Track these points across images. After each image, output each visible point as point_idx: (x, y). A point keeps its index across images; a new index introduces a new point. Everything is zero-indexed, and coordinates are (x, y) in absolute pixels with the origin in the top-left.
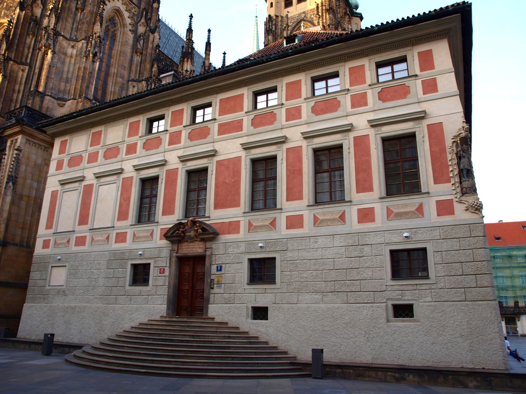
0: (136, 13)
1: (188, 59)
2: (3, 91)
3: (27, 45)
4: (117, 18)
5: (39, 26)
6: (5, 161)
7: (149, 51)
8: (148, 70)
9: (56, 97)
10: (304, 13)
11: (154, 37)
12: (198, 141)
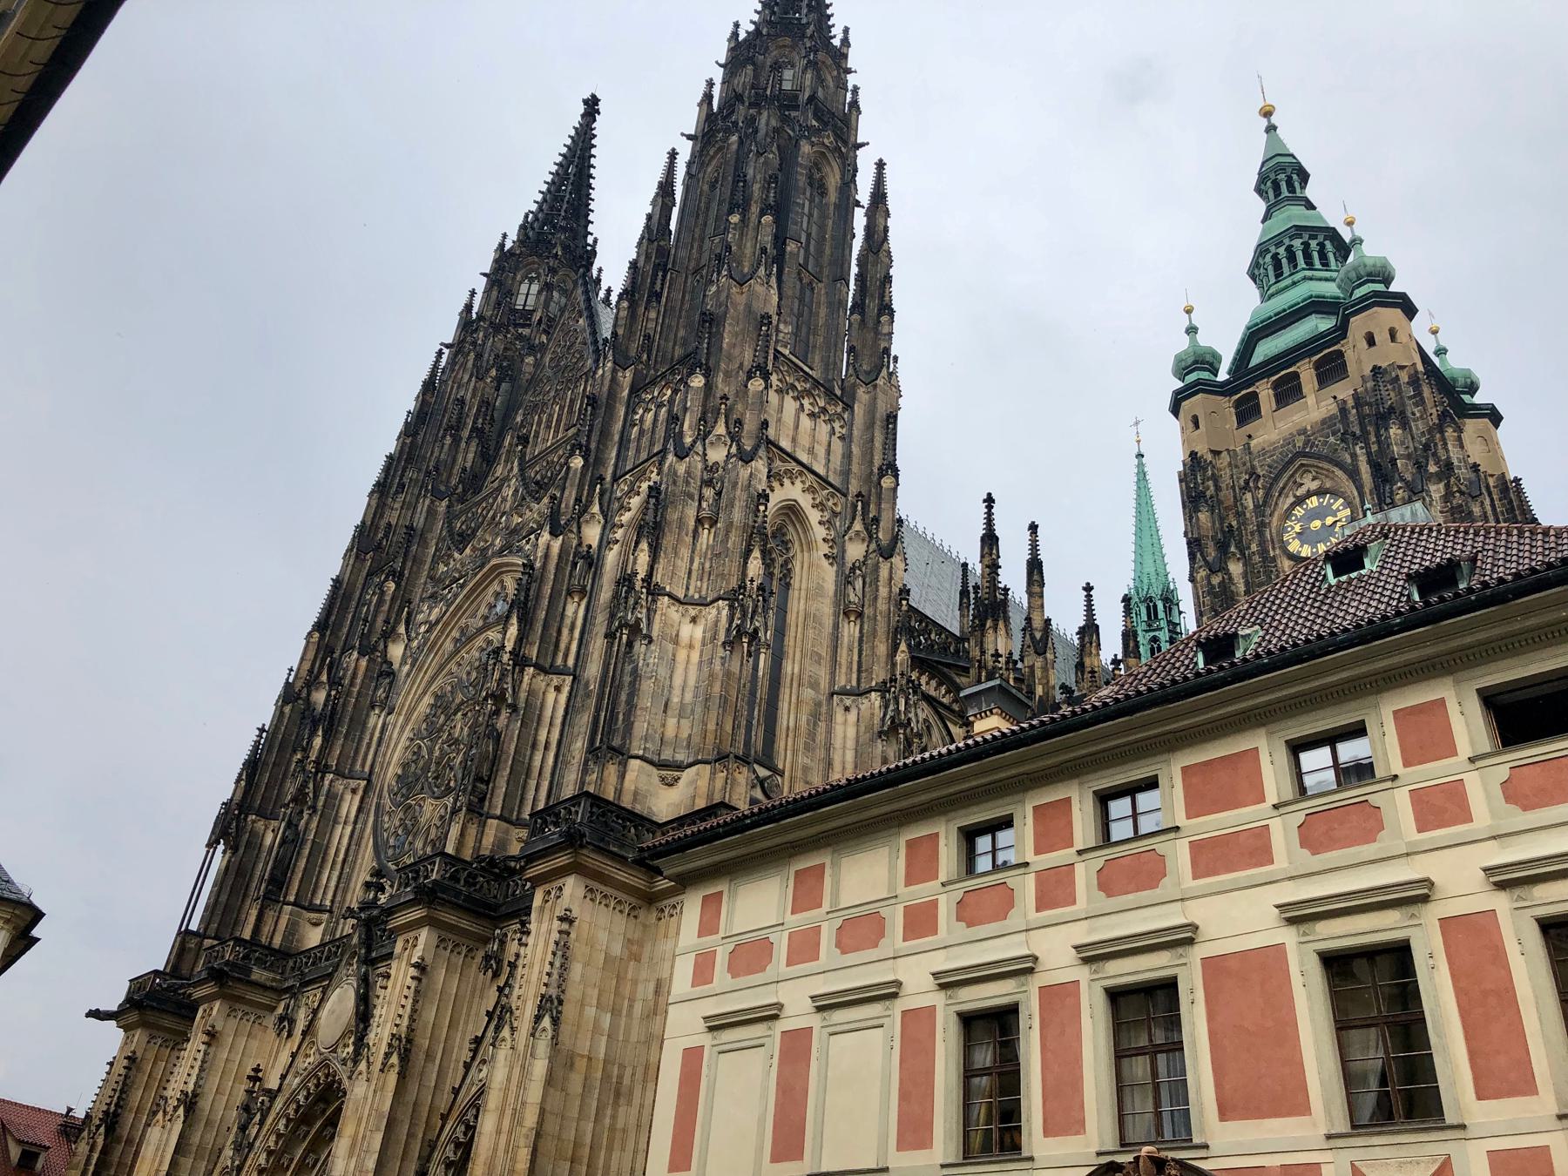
0: (838, 509)
1: (996, 621)
4: (791, 528)
7: (882, 605)
8: (883, 659)
9: (656, 758)
10: (1303, 432)
12: (1130, 897)
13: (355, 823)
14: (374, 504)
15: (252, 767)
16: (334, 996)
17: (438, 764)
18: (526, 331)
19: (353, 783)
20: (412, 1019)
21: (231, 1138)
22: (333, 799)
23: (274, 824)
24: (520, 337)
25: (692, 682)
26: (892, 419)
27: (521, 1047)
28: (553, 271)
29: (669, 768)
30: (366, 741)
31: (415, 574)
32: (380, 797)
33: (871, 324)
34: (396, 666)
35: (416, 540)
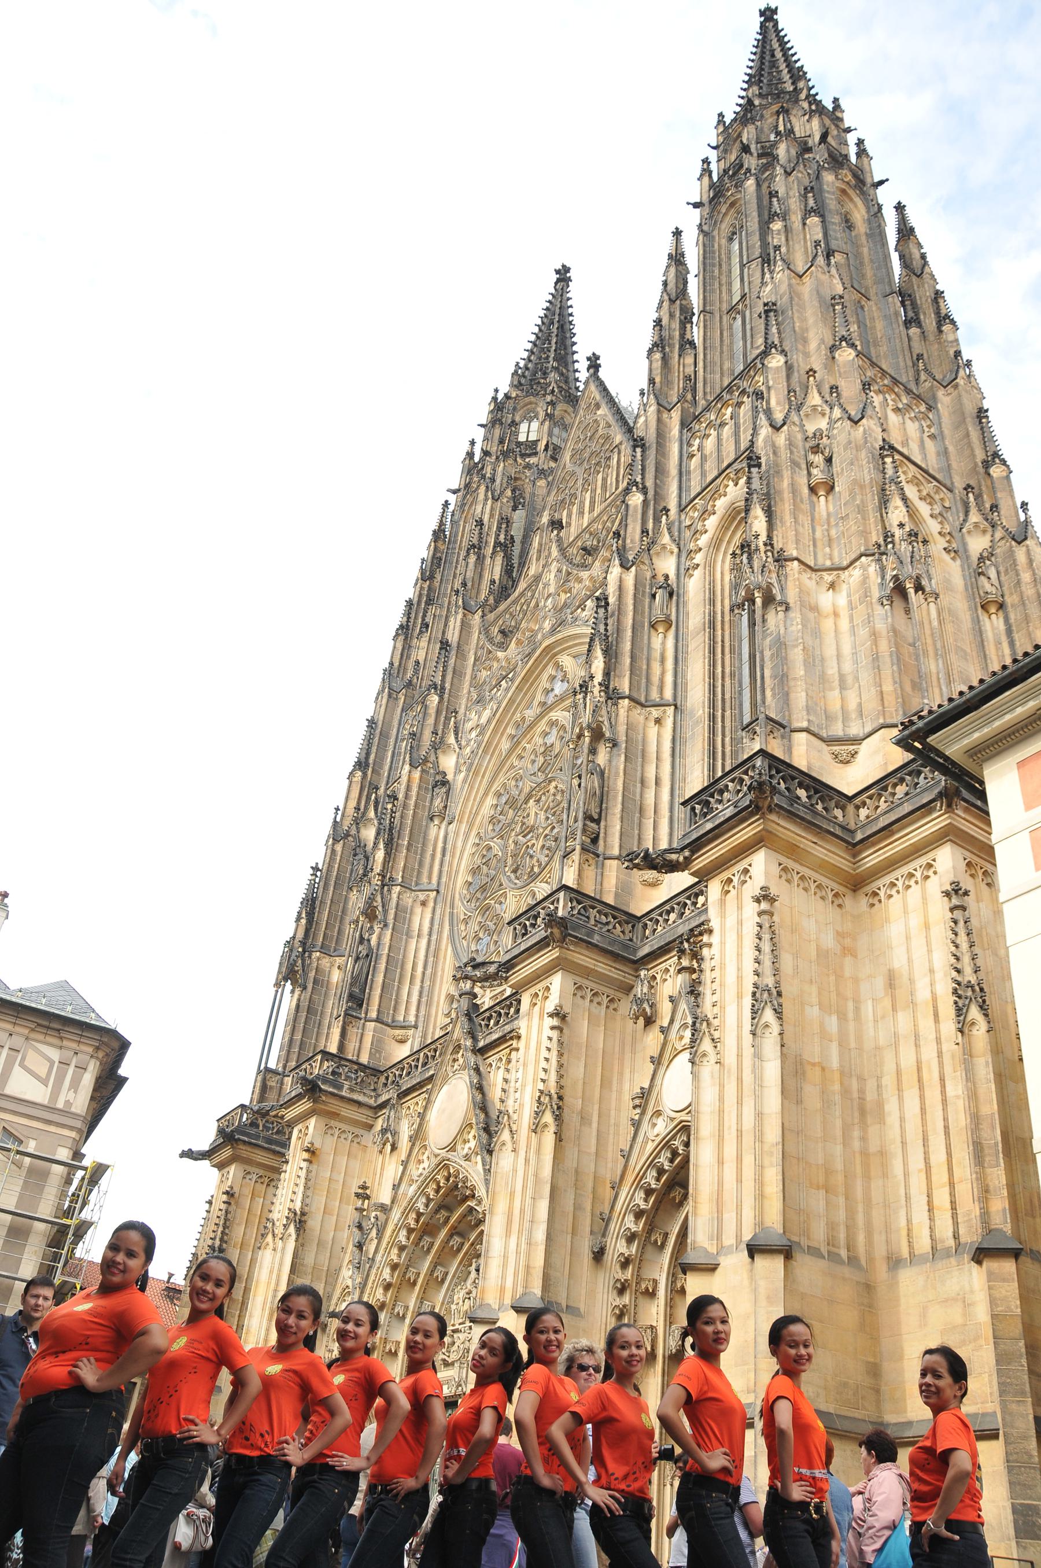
0: (947, 505)
5: (678, 596)
6: (715, 950)
11: (1028, 552)
13: (430, 935)
14: (400, 646)
15: (310, 905)
17: (514, 856)
18: (533, 460)
19: (422, 896)
23: (339, 961)
24: (528, 466)
25: (847, 649)
26: (981, 414)
28: (552, 403)
30: (430, 852)
31: (456, 688)
32: (452, 906)
34: (450, 777)
35: (453, 652)
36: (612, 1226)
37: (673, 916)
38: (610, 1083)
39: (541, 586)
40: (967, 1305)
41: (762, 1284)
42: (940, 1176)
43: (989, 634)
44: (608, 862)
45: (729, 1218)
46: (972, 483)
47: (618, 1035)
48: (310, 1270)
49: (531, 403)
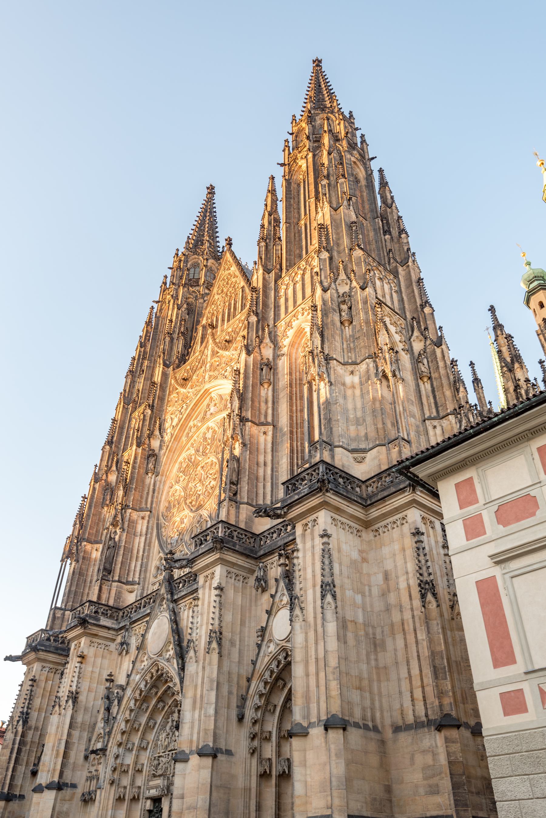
0: (403, 326)
2: (245, 465)
3: (263, 399)
5: (274, 370)
6: (300, 561)
7: (442, 371)
13: (146, 535)
16: (154, 625)
19: (142, 514)
20: (221, 621)
21: (101, 716)
22: (132, 523)
26: (420, 281)
27: (311, 619)
29: (358, 452)
32: (158, 519)
33: (395, 240)
34: (157, 451)
36: (248, 703)
37: (275, 535)
38: (245, 622)
39: (204, 357)
40: (435, 755)
41: (332, 747)
42: (417, 682)
43: (423, 392)
44: (241, 506)
45: (313, 707)
46: (415, 316)
47: (248, 596)
48: (79, 725)
49: (195, 258)
